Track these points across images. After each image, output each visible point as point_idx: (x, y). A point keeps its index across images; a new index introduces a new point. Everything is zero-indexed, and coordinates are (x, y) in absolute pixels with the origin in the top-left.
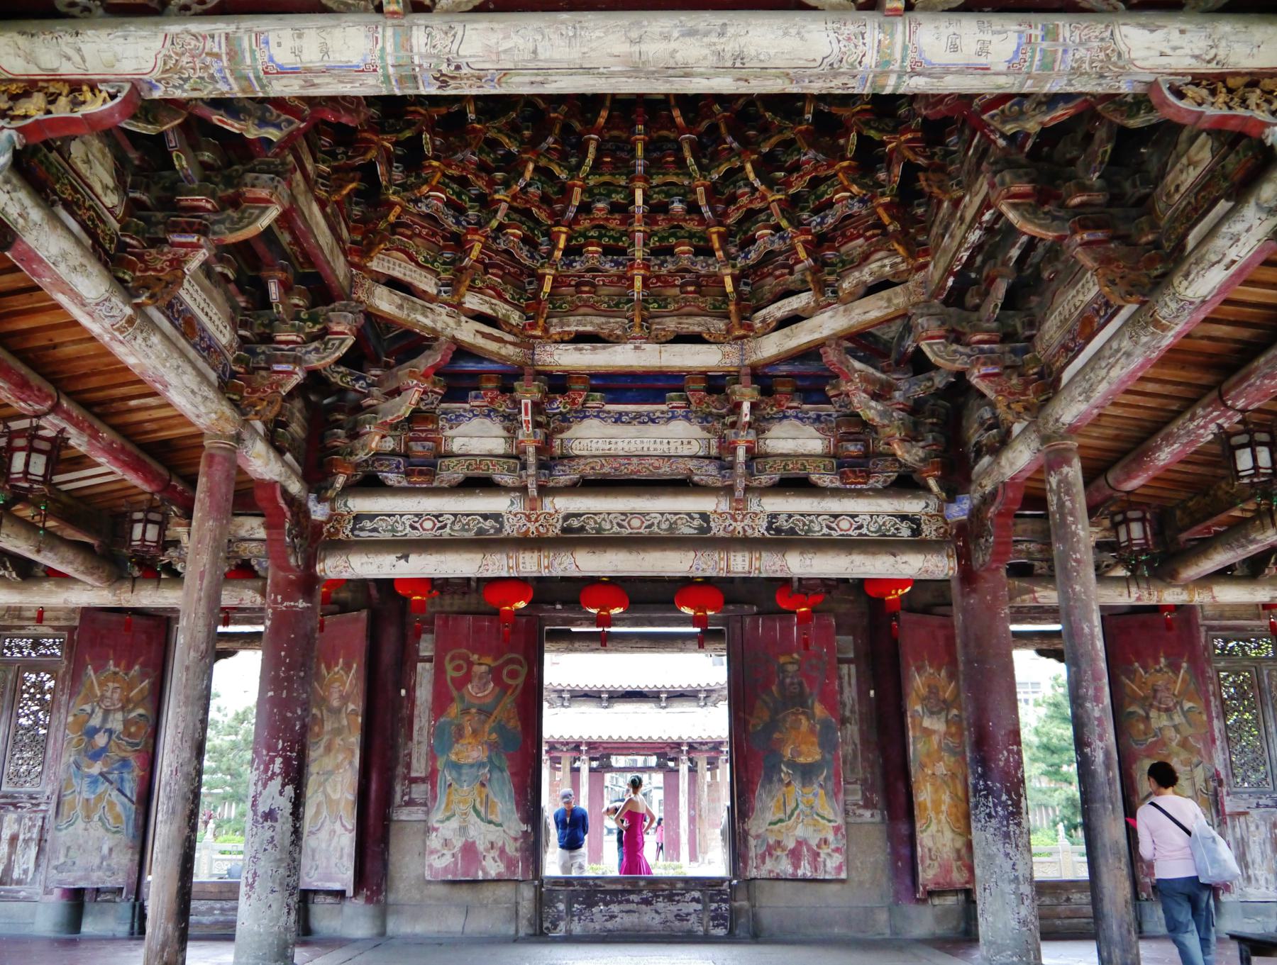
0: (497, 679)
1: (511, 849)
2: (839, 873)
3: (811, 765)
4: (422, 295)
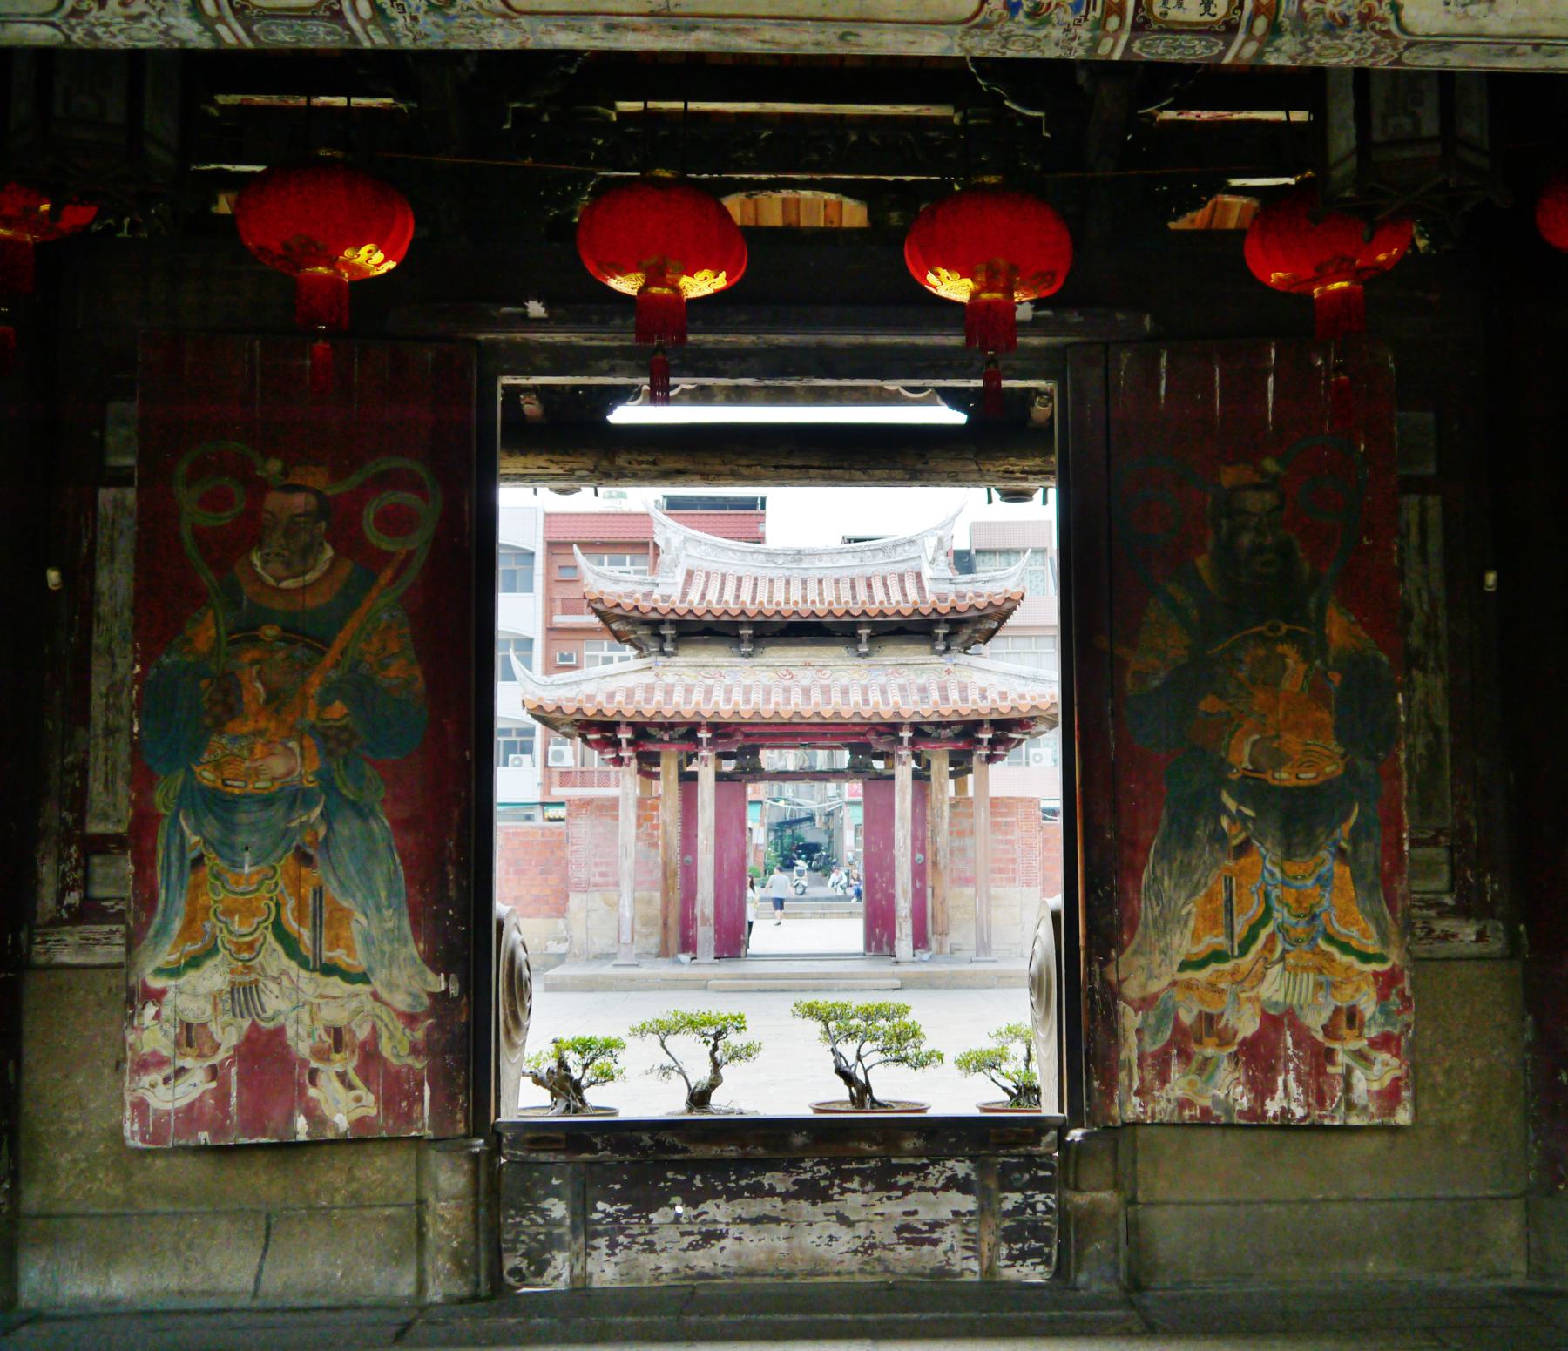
0: (347, 538)
1: (396, 1049)
2: (1391, 1111)
3: (1312, 791)
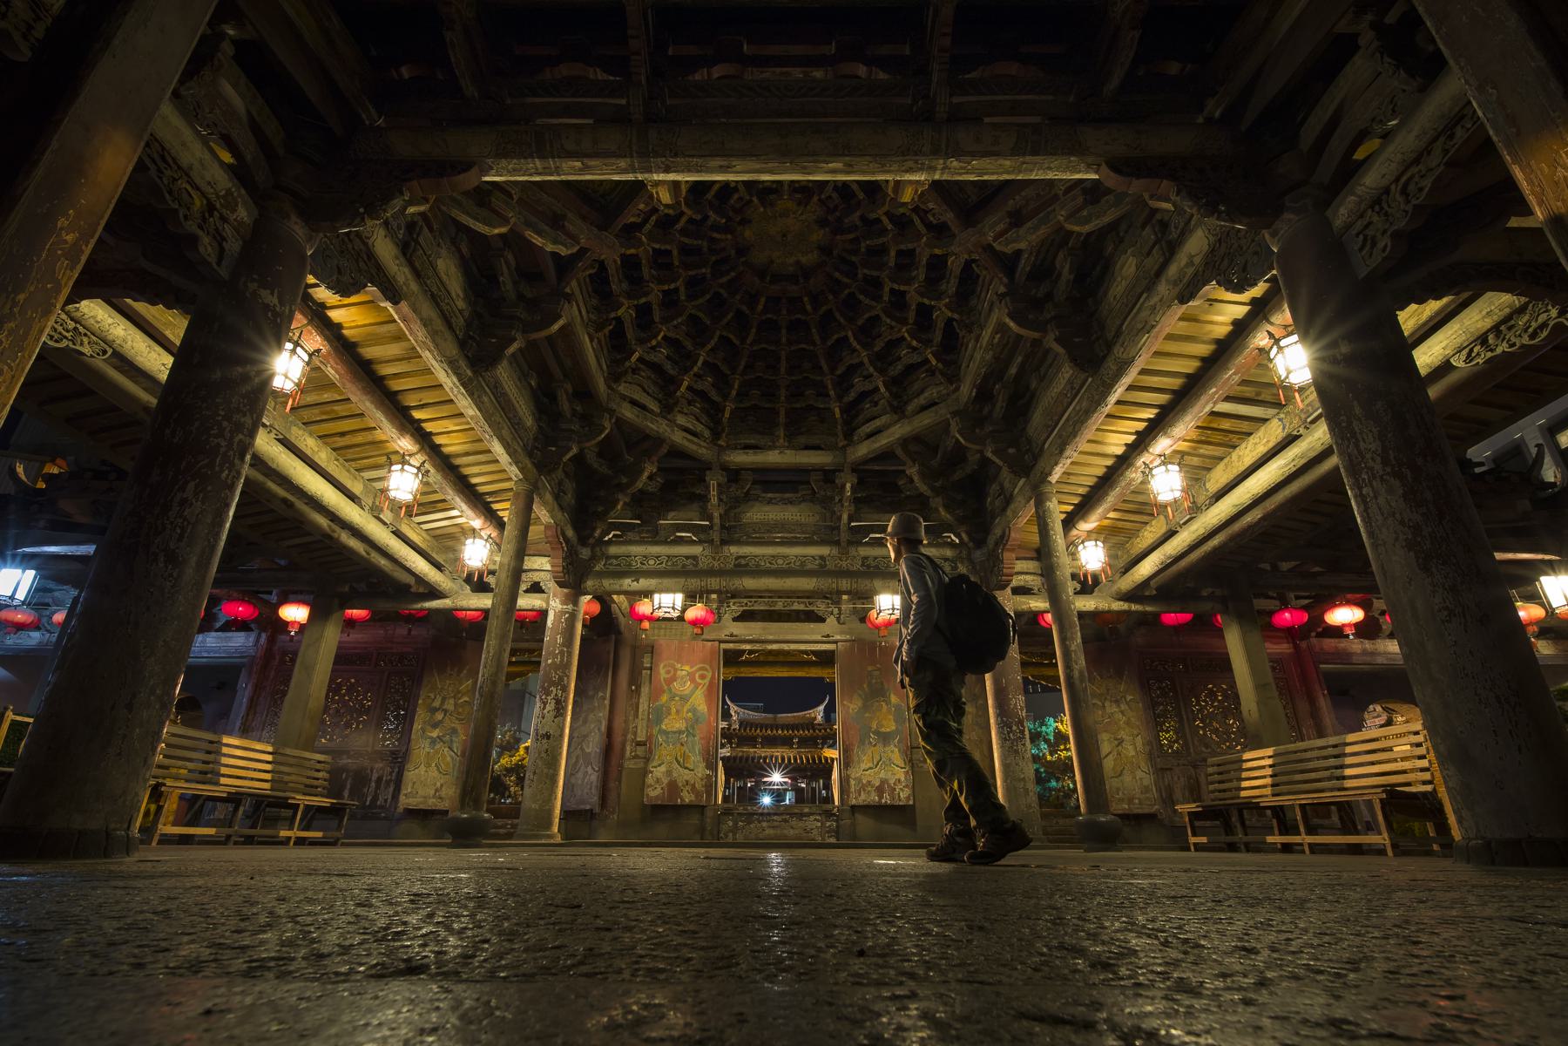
0: (693, 680)
4: (651, 412)
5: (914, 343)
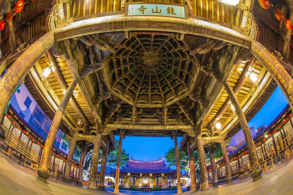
5: (179, 80)
